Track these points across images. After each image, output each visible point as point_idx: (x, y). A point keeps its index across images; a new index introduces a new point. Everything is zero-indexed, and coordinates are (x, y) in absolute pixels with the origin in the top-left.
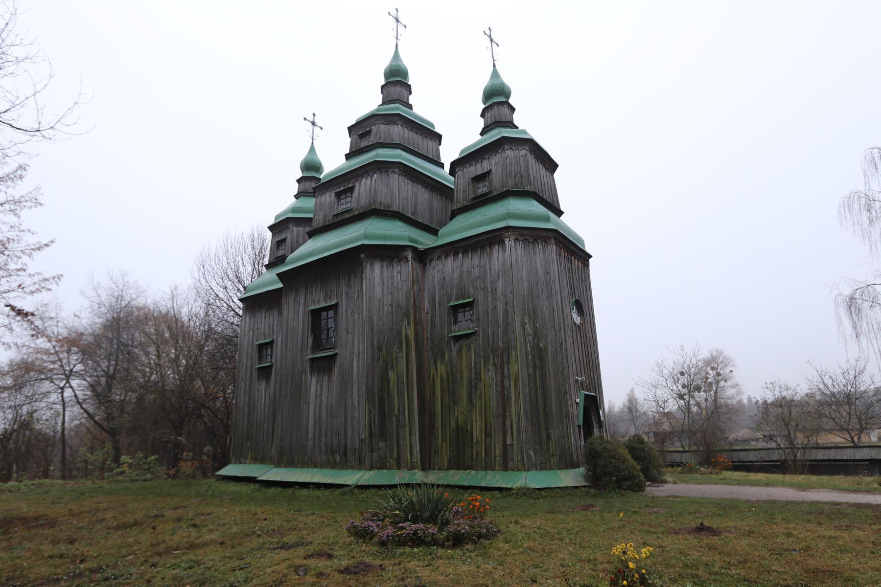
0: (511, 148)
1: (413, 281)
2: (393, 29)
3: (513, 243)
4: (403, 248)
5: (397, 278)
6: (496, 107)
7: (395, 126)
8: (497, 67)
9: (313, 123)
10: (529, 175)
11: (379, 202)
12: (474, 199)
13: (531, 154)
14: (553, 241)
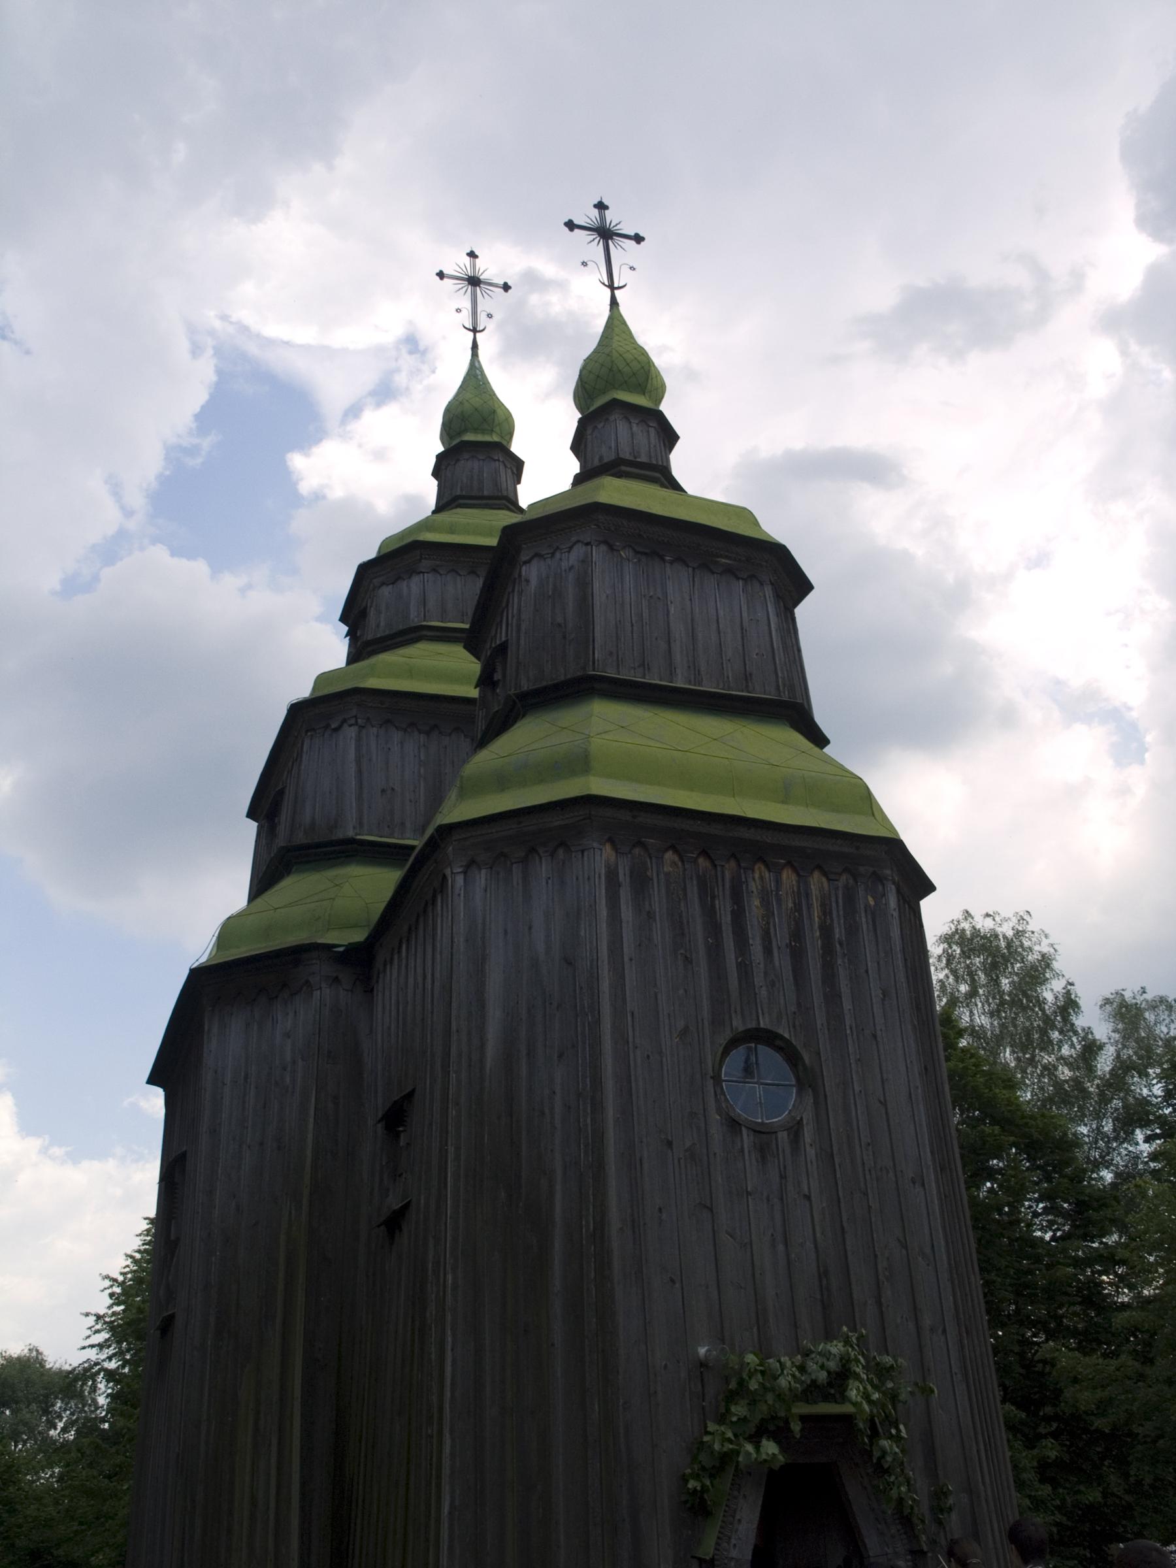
0: (537, 555)
2: (458, 310)
3: (460, 880)
6: (589, 431)
7: (416, 579)
8: (624, 310)
13: (611, 548)
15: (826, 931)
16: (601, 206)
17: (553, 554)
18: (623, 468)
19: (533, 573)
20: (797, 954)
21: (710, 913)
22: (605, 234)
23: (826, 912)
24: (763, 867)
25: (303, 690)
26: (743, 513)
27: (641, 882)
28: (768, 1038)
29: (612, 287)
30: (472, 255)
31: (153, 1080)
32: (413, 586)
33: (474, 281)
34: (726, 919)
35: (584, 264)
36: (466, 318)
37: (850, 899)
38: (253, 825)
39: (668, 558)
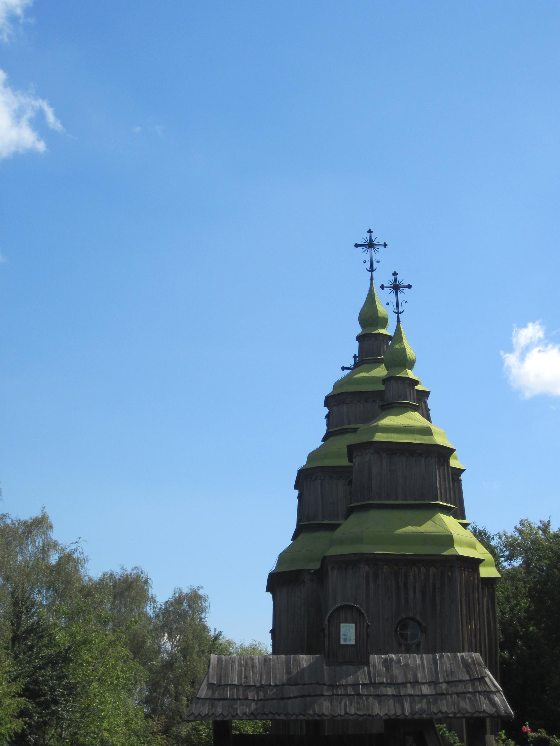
2: (364, 262)
4: (299, 573)
17: (362, 456)
18: (394, 405)
24: (415, 567)
25: (302, 462)
28: (413, 619)
29: (398, 313)
30: (370, 232)
31: (267, 591)
33: (371, 245)
35: (388, 304)
36: (367, 266)
39: (398, 454)
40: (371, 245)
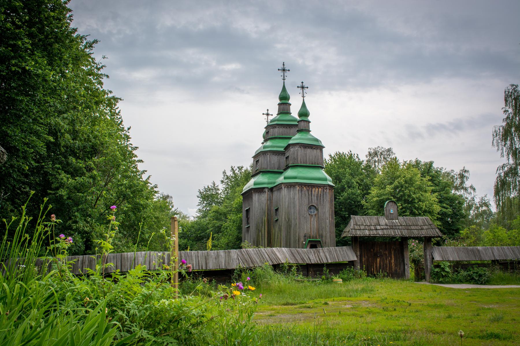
1: (267, 200)
4: (264, 188)
5: (263, 199)
9: (268, 114)
10: (297, 158)
11: (263, 167)
12: (286, 166)
14: (297, 186)
15: (321, 194)
16: (302, 83)
19: (292, 150)
20: (317, 197)
21: (308, 193)
22: (303, 87)
23: (321, 192)
26: (317, 140)
27: (302, 191)
29: (303, 97)
32: (276, 130)
33: (284, 70)
34: (310, 194)
36: (282, 77)
37: (323, 191)
38: (253, 159)
40: (284, 70)
